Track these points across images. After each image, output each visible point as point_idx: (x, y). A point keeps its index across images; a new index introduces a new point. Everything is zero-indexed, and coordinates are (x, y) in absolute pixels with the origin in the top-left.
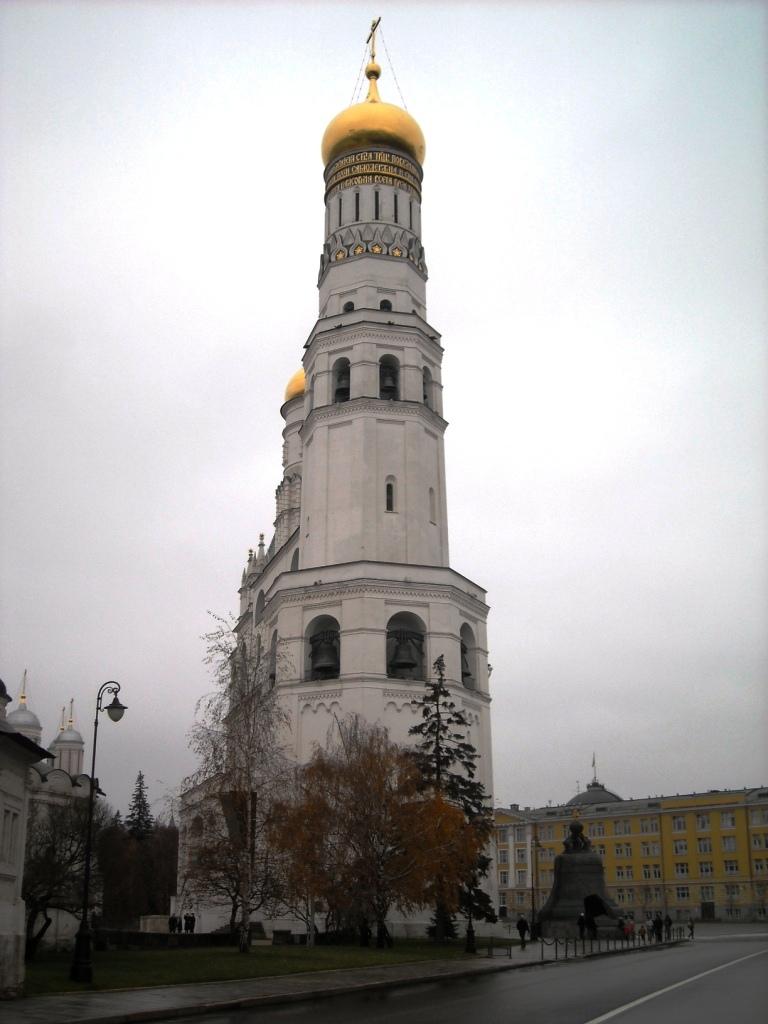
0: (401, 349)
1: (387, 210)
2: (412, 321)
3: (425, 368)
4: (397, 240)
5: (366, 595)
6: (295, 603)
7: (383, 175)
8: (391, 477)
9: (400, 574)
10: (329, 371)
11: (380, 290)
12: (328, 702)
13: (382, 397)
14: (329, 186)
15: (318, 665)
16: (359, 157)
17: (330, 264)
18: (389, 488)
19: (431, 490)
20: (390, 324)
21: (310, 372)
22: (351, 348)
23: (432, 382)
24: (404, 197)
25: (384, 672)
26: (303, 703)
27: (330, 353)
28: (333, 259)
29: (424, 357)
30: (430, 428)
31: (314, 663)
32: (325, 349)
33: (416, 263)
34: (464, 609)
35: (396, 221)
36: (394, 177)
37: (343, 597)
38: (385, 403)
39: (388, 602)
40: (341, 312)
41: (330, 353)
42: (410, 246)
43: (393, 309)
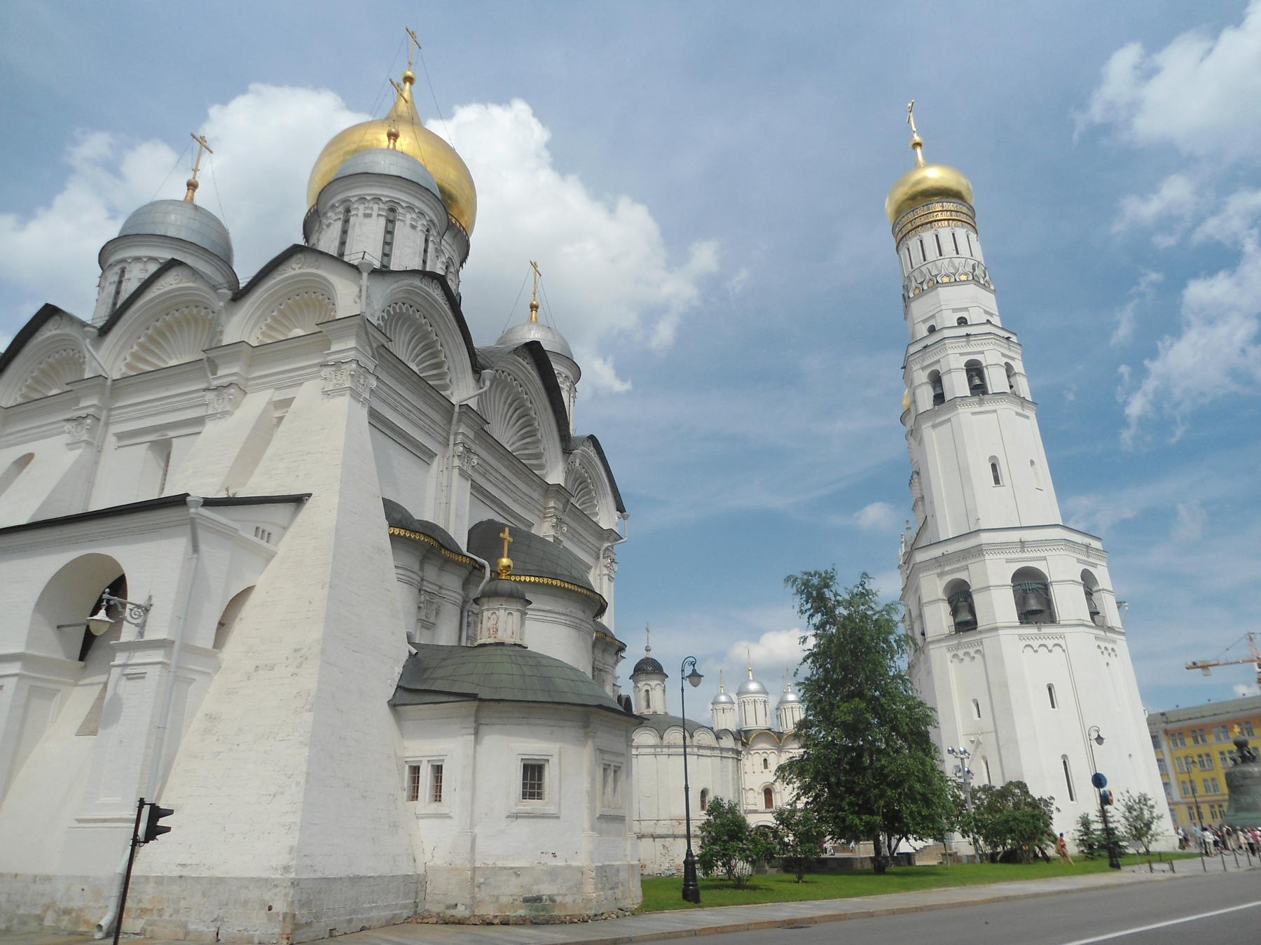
0: (982, 352)
3: (1007, 364)
7: (939, 220)
9: (1015, 536)
11: (955, 310)
12: (972, 651)
13: (973, 395)
14: (898, 240)
15: (958, 620)
16: (917, 212)
17: (910, 300)
19: (1032, 462)
20: (968, 335)
21: (910, 387)
22: (938, 361)
24: (961, 233)
29: (1004, 355)
30: (1020, 411)
31: (954, 620)
32: (918, 366)
33: (982, 282)
35: (958, 253)
36: (948, 220)
37: (969, 562)
38: (976, 399)
39: (1008, 561)
42: (974, 270)
43: (969, 323)
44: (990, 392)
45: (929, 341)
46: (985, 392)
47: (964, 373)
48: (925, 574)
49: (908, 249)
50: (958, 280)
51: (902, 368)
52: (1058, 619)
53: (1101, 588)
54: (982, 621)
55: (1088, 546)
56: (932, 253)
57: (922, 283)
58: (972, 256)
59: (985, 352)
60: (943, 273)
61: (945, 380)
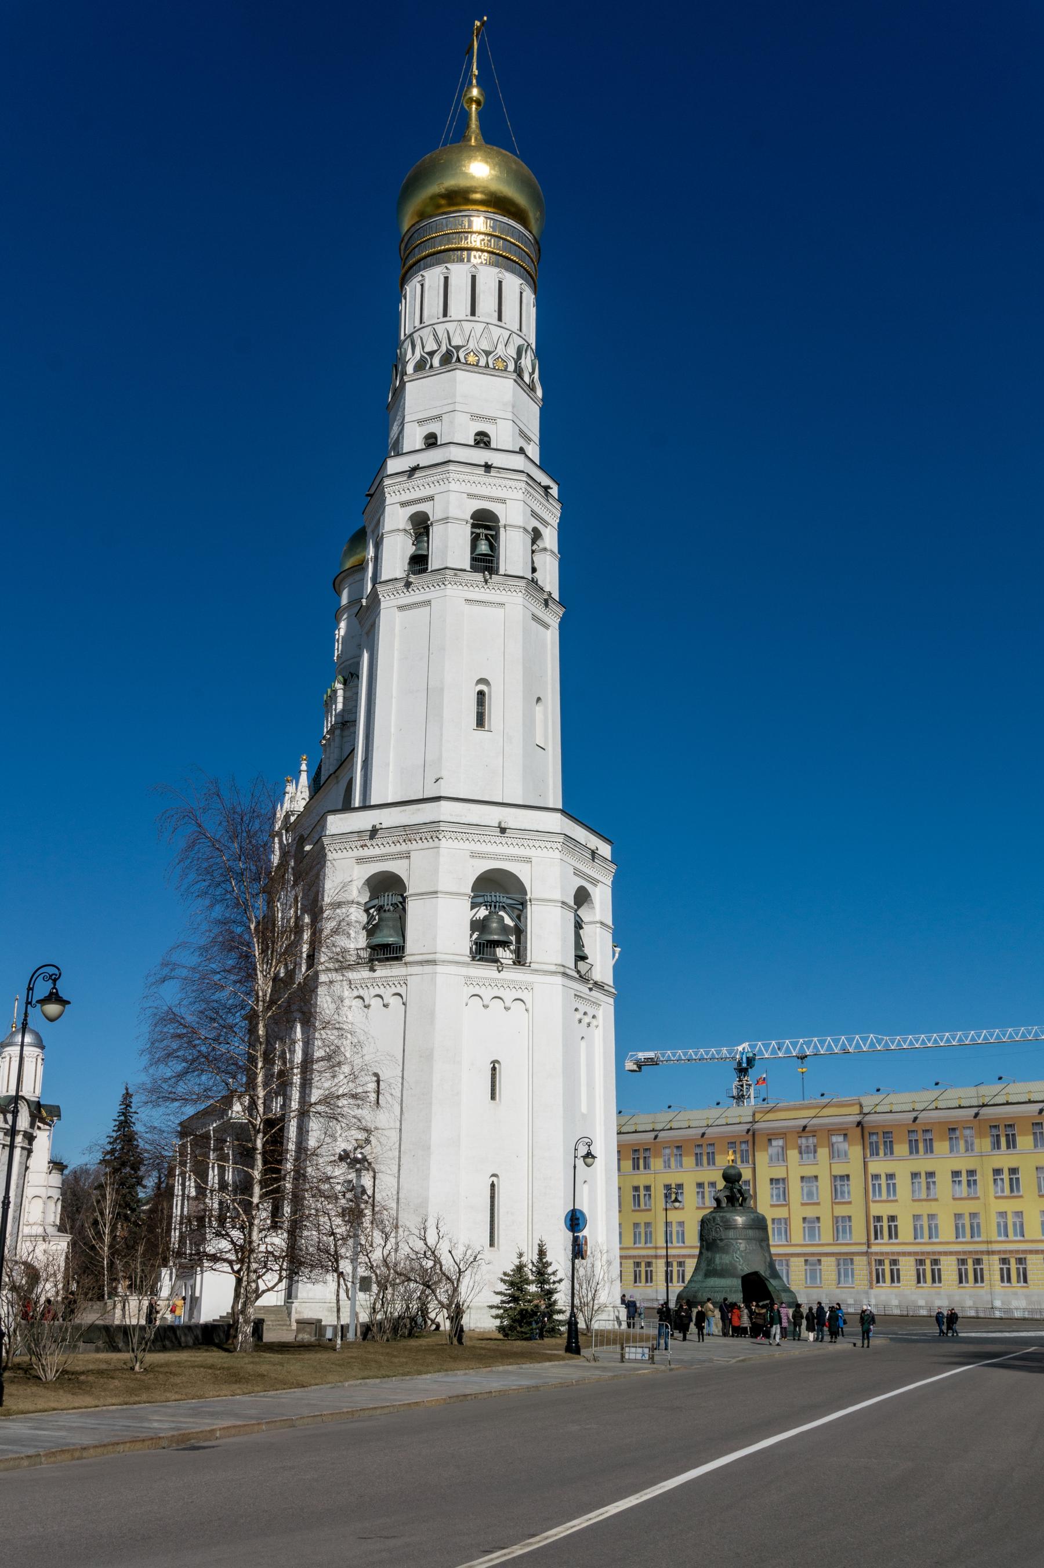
0: (503, 501)
1: (487, 304)
4: (501, 346)
9: (493, 816)
11: (476, 417)
13: (474, 569)
22: (431, 498)
27: (403, 504)
29: (534, 514)
35: (500, 319)
38: (479, 577)
39: (474, 855)
41: (403, 504)
43: (493, 445)
44: (502, 572)
47: (468, 529)
49: (422, 285)
50: (491, 366)
52: (528, 961)
54: (414, 945)
56: (459, 306)
57: (431, 354)
58: (521, 331)
60: (471, 345)
61: (436, 532)
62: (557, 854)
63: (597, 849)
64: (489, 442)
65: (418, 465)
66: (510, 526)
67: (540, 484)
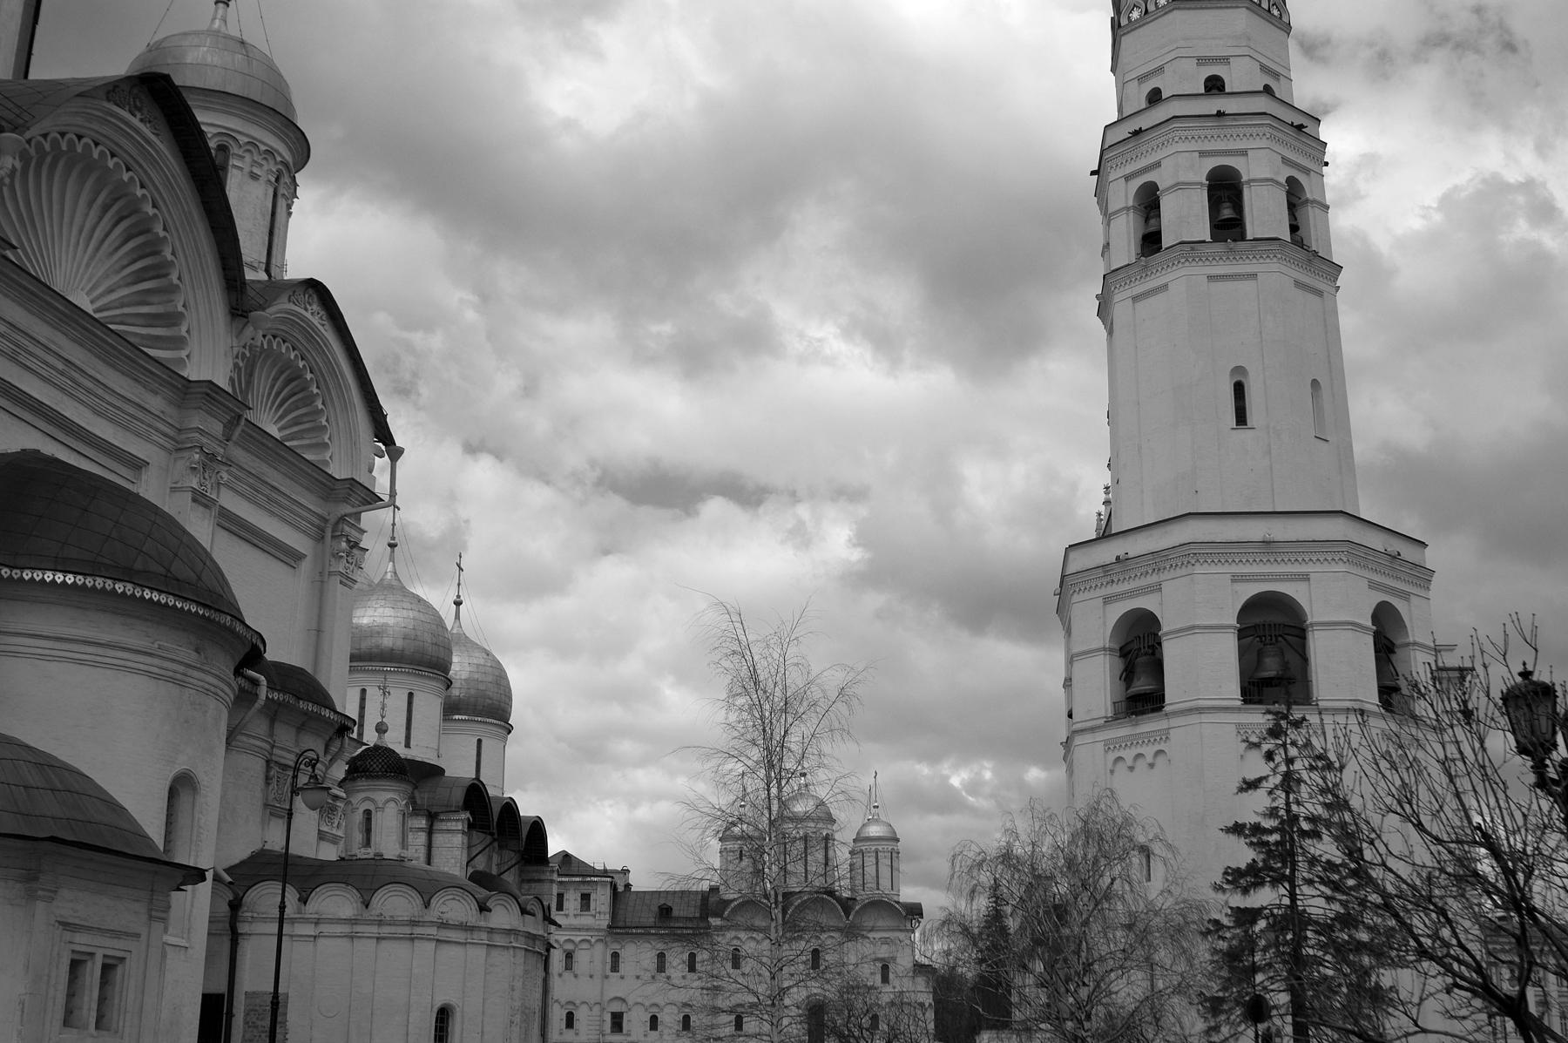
0: (1244, 153)
2: (1261, 104)
3: (1292, 183)
5: (1198, 569)
6: (1092, 594)
8: (1239, 370)
9: (1255, 530)
10: (1128, 209)
11: (1202, 61)
12: (1149, 751)
15: (1133, 690)
18: (1239, 389)
19: (1315, 384)
20: (1220, 114)
22: (1158, 164)
23: (1307, 201)
25: (1238, 695)
26: (1112, 756)
27: (1128, 178)
28: (1124, 22)
29: (1286, 161)
31: (1127, 689)
34: (1377, 578)
37: (1163, 576)
39: (1236, 579)
40: (1144, 106)
41: (1128, 178)
43: (1227, 90)
44: (1249, 236)
45: (1144, 122)
46: (1242, 237)
48: (1082, 596)
51: (1093, 173)
53: (1411, 639)
55: (1395, 557)
59: (1250, 152)
62: (1341, 567)
63: (1399, 554)
64: (1224, 87)
65: (1141, 128)
66: (1254, 180)
67: (1292, 125)
